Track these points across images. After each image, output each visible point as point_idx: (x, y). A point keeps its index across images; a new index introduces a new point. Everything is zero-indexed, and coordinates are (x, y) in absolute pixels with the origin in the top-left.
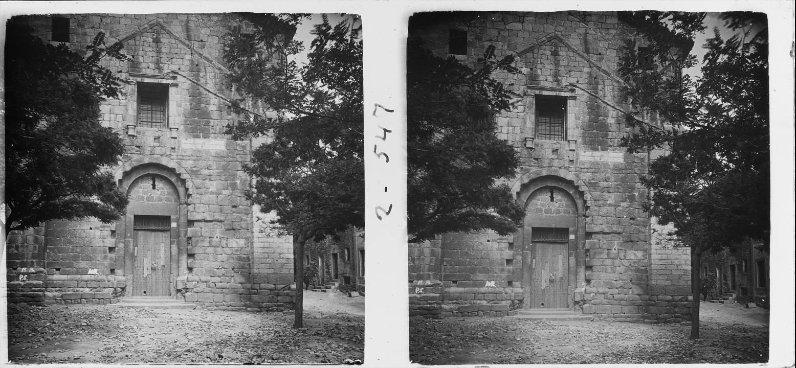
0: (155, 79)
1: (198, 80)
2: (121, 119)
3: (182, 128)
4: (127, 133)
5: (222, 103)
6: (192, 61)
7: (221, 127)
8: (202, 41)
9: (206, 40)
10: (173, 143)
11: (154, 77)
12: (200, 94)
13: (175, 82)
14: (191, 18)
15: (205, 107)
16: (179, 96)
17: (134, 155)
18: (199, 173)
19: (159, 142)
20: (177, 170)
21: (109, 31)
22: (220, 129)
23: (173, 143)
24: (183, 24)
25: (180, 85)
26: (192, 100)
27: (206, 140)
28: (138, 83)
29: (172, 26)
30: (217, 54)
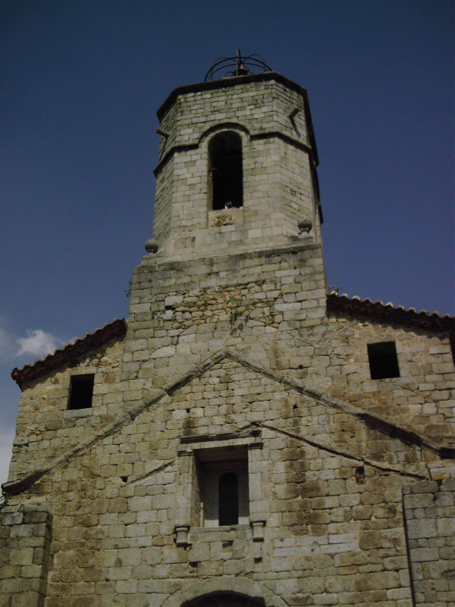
0: (224, 441)
1: (298, 431)
2: (165, 517)
3: (273, 520)
4: (175, 540)
5: (345, 465)
6: (286, 401)
7: (348, 509)
8: (301, 367)
9: (307, 365)
10: (256, 549)
11: (221, 437)
12: (303, 453)
13: (258, 440)
14: (282, 337)
15: (314, 475)
16: (265, 463)
17: (187, 580)
18: (309, 601)
19: (232, 550)
20: (267, 599)
21: (151, 379)
22: (345, 511)
23: (256, 549)
24: (268, 348)
25: (266, 444)
26: (291, 466)
27: (222, 546)
28: (196, 452)
29: (251, 354)
30: (330, 384)
